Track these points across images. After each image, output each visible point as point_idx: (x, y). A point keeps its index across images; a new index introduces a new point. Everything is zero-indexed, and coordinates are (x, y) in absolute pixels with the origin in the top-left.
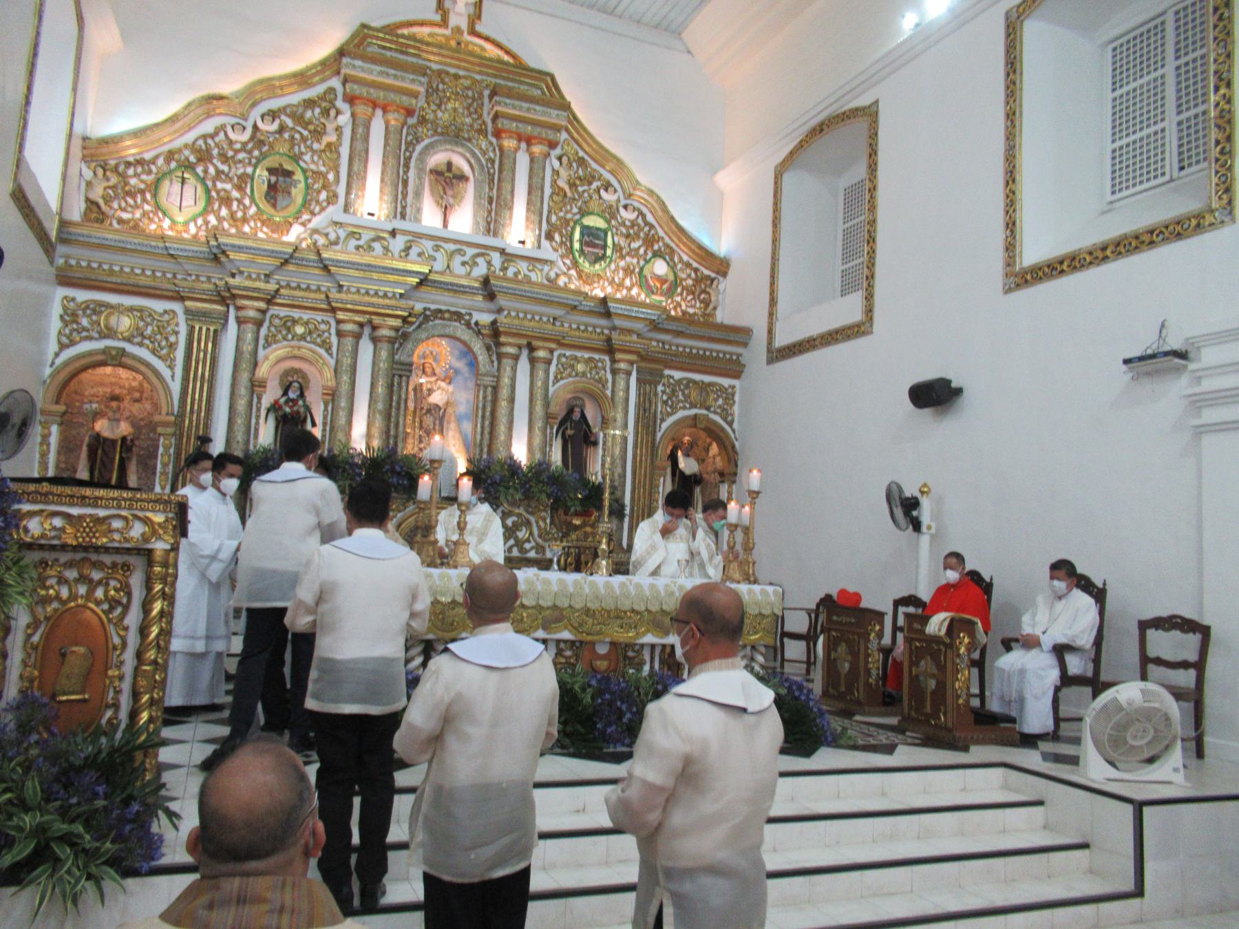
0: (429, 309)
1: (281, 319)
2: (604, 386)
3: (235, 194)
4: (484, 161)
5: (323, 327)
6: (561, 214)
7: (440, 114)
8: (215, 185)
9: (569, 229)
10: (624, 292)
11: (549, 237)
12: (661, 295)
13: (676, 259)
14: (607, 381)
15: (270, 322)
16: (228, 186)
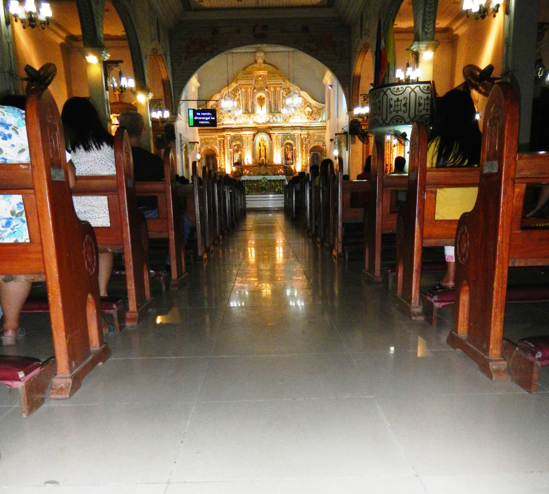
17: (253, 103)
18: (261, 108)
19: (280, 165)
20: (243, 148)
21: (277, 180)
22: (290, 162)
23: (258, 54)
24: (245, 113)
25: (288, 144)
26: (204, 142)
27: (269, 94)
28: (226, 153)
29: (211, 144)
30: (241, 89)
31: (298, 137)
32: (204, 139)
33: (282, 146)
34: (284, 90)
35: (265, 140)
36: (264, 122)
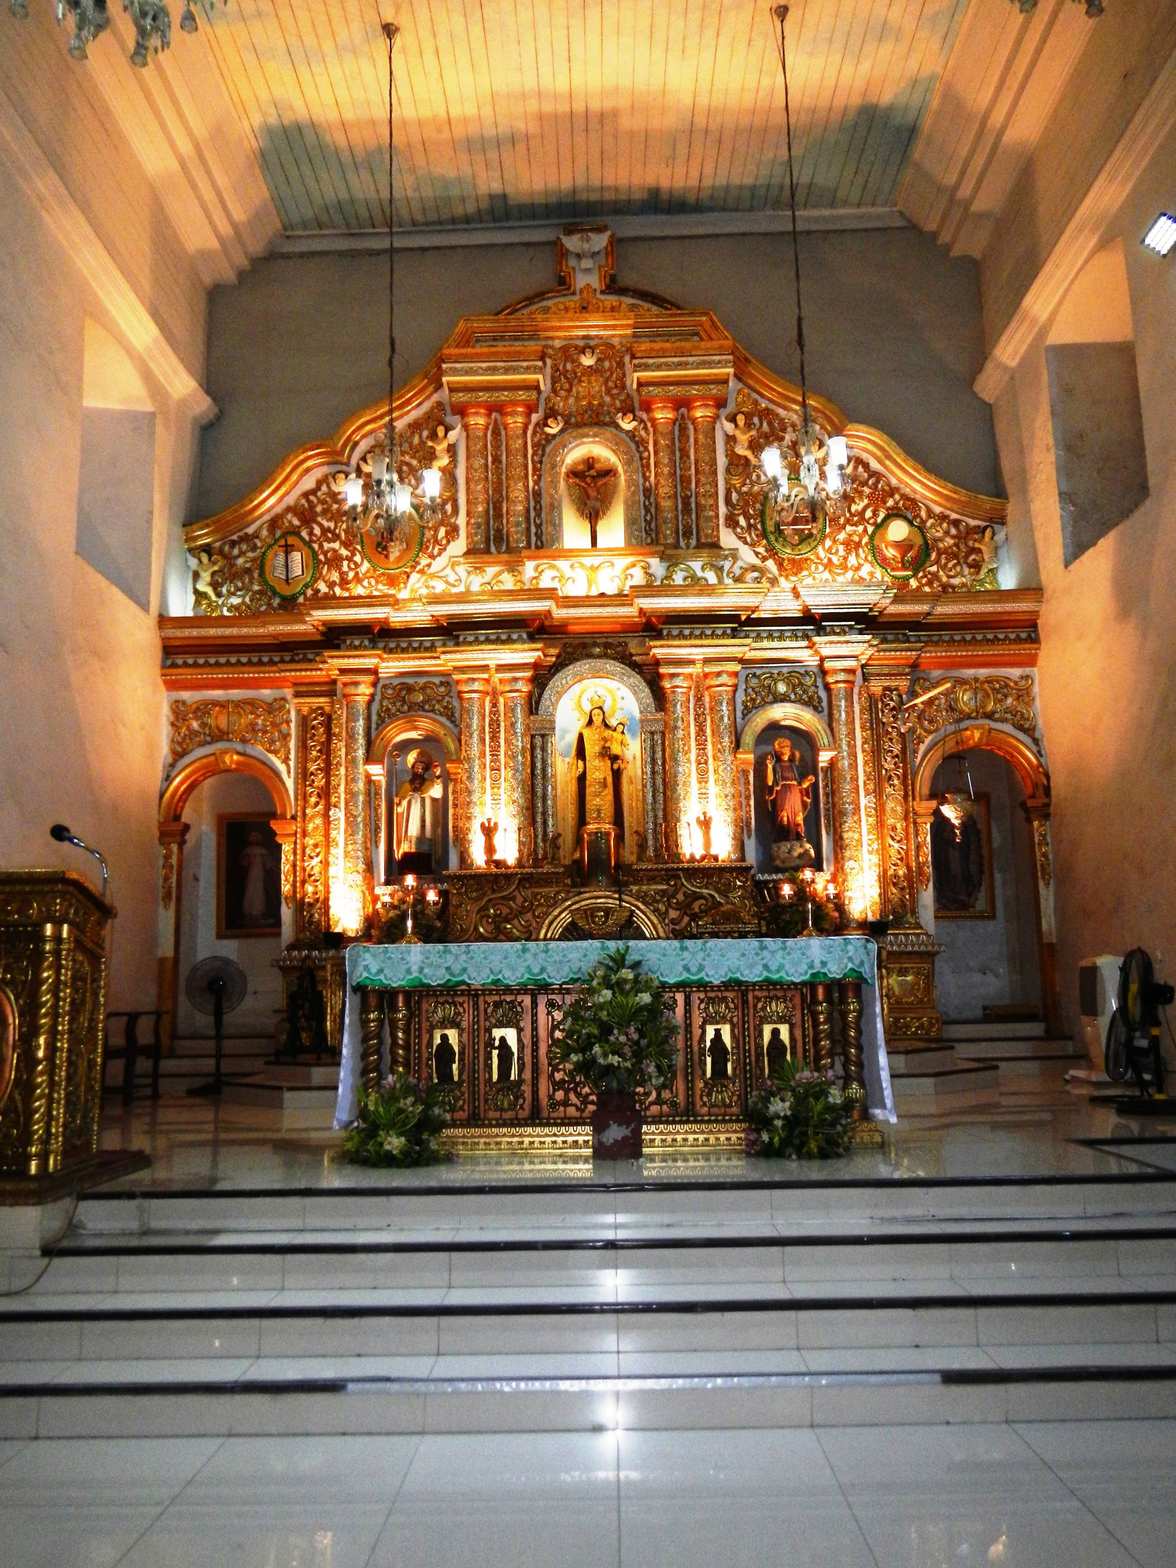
0: (571, 645)
1: (394, 688)
2: (815, 709)
3: (344, 552)
4: (633, 446)
5: (442, 689)
6: (745, 489)
7: (571, 401)
8: (321, 546)
9: (758, 506)
10: (850, 574)
11: (732, 522)
12: (904, 568)
13: (923, 514)
14: (819, 698)
15: (382, 694)
16: (336, 545)
17: (537, 495)
18: (587, 526)
19: (731, 870)
20: (459, 761)
21: (773, 988)
22: (799, 851)
23: (572, 243)
24: (487, 551)
25: (774, 729)
26: (195, 725)
27: (640, 444)
28: (340, 794)
29: (244, 741)
30: (461, 411)
31: (852, 683)
32: (202, 710)
33: (737, 745)
34: (741, 419)
35: (613, 722)
36: (611, 590)
